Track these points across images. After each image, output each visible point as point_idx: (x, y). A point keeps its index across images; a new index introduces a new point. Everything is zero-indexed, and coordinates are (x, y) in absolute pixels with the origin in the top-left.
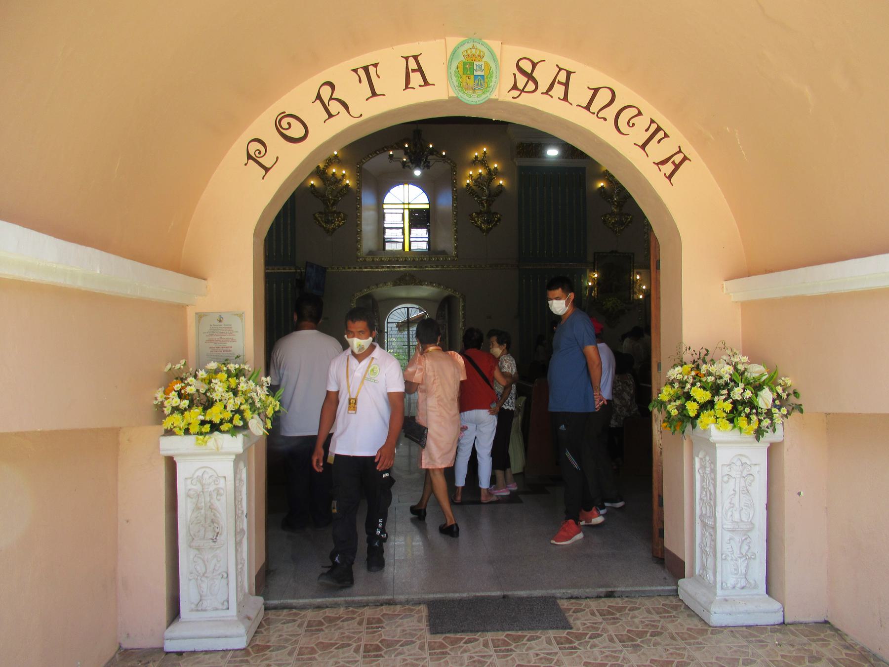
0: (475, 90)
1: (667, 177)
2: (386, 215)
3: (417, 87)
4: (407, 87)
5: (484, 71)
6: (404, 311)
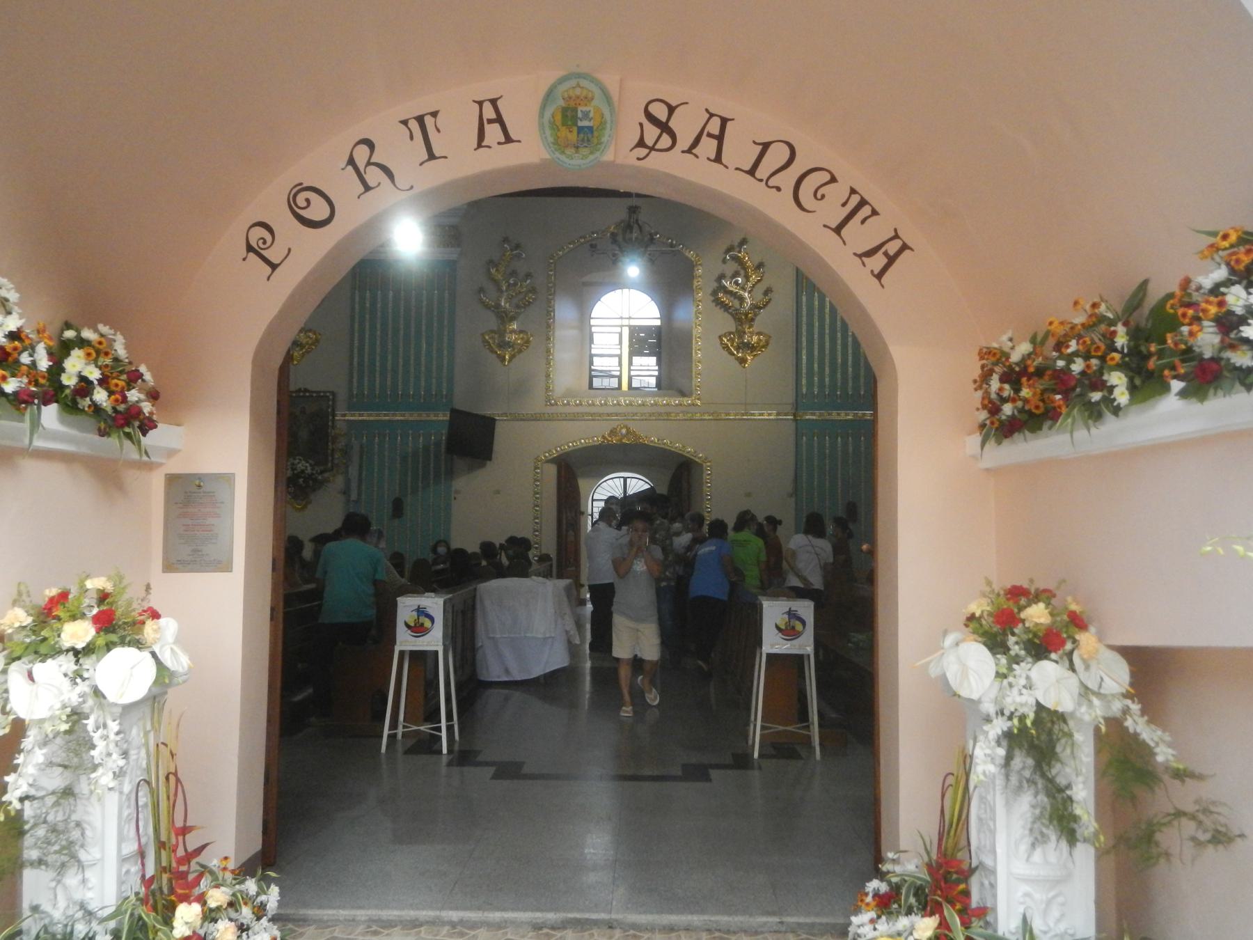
0: (579, 149)
1: (874, 276)
2: (596, 337)
3: (494, 145)
4: (480, 146)
5: (592, 121)
6: (619, 483)
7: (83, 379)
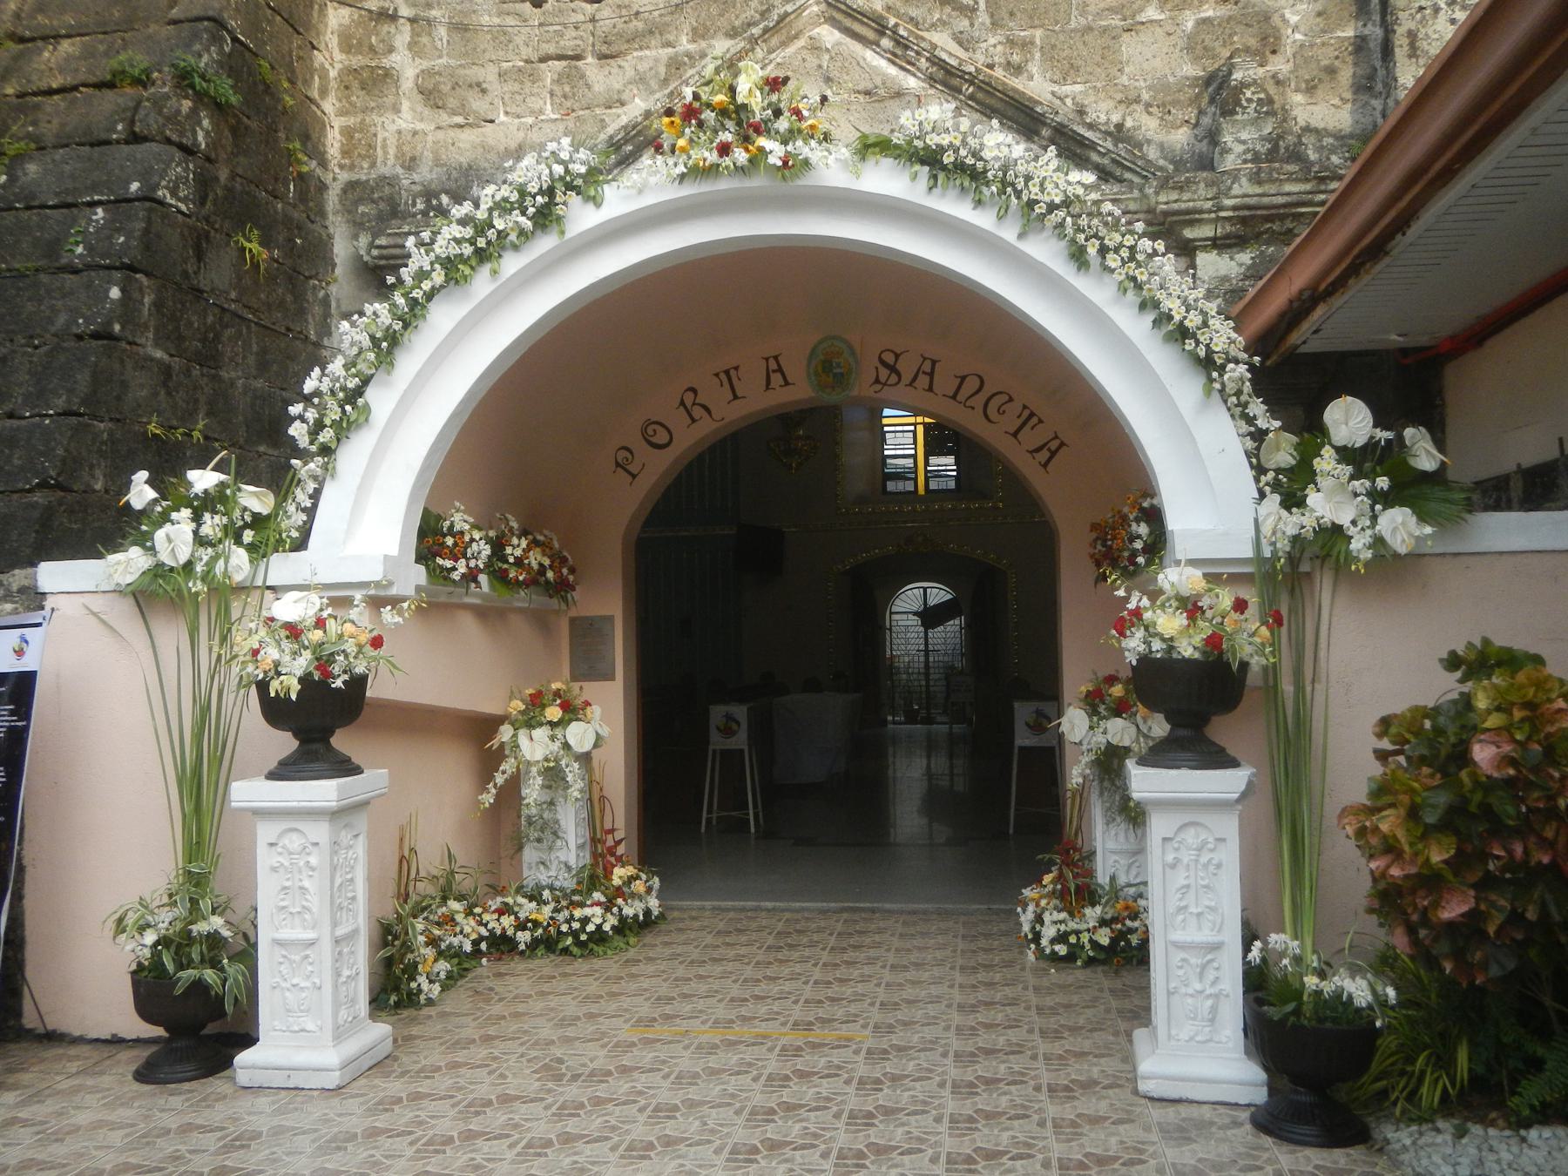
7: (541, 565)
